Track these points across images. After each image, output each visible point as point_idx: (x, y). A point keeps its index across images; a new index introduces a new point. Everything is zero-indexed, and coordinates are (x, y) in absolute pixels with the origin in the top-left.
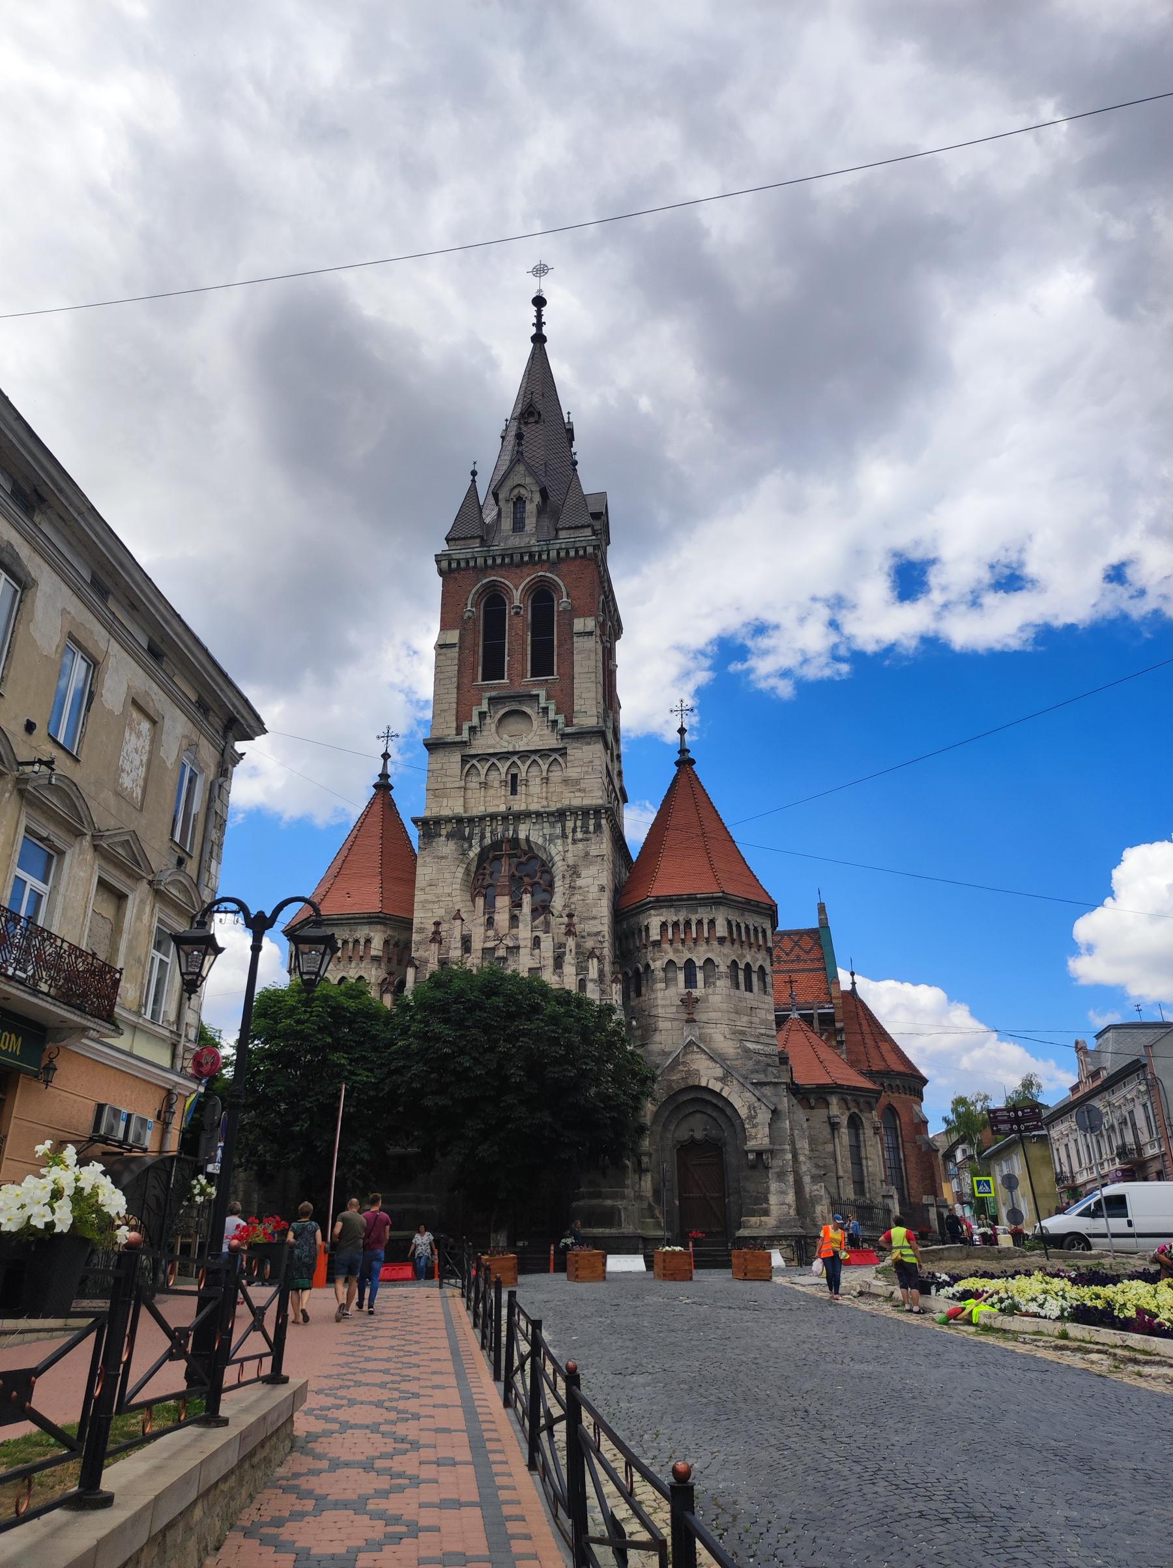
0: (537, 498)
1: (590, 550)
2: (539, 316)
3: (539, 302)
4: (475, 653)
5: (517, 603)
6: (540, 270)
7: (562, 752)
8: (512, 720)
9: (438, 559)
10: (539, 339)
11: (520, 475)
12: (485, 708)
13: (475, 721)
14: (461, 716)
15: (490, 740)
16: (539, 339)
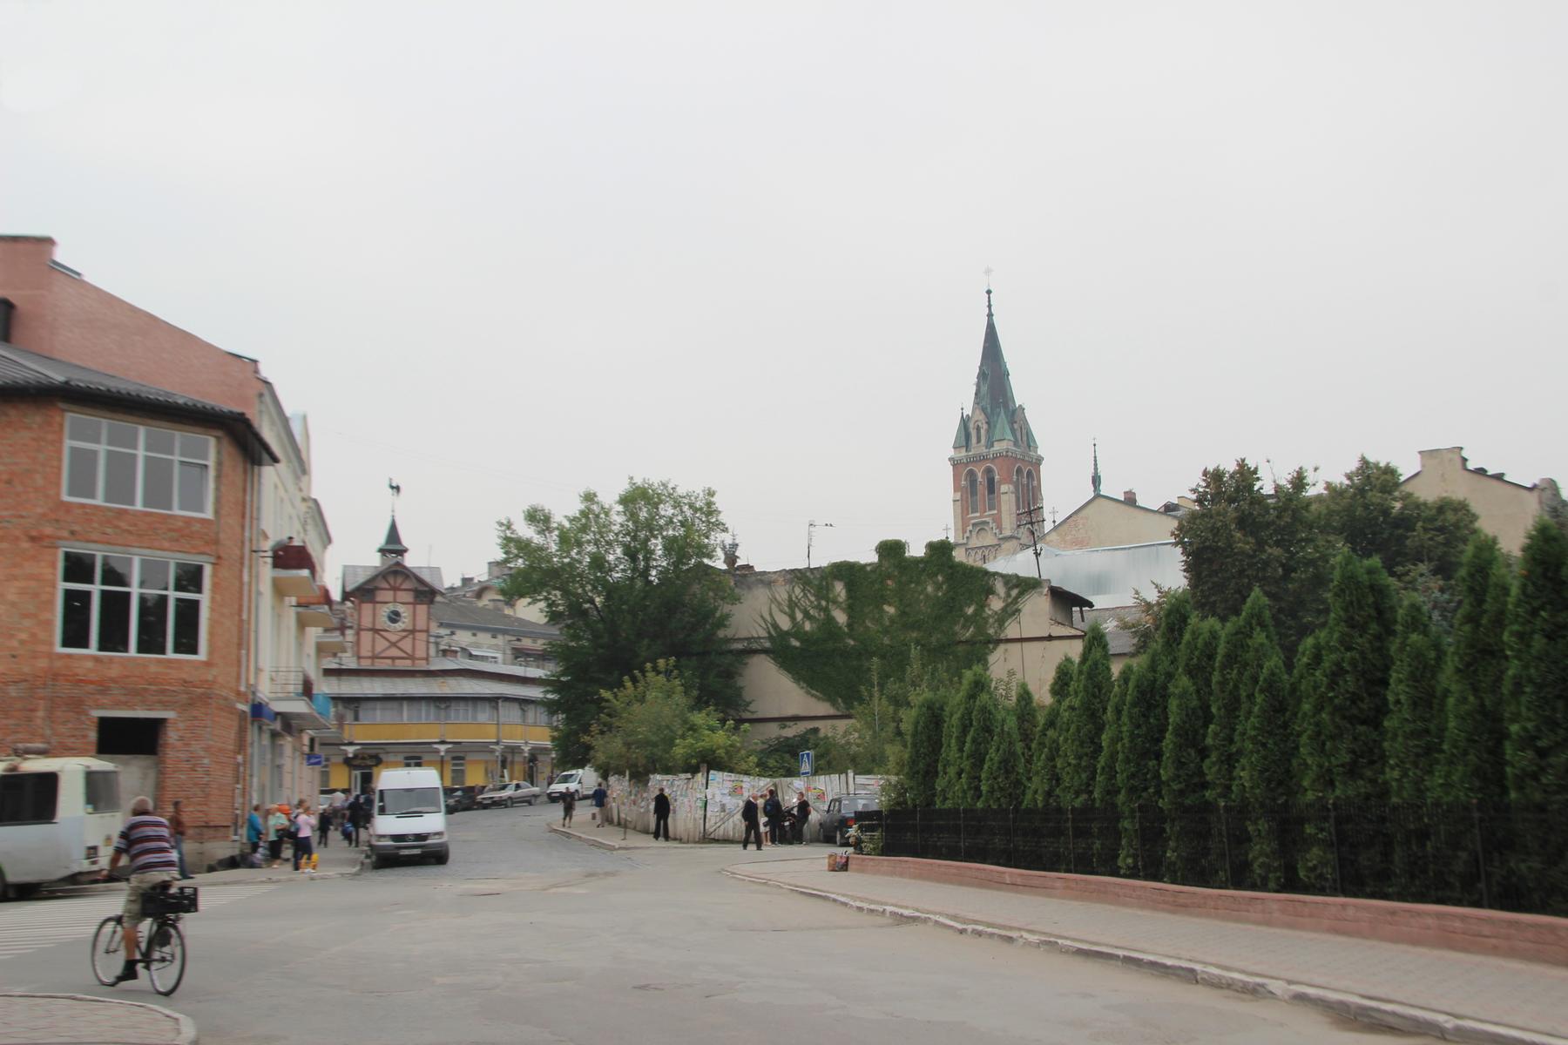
0: (985, 426)
1: (1004, 453)
2: (989, 301)
3: (989, 292)
4: (967, 502)
5: (980, 479)
6: (988, 271)
7: (999, 545)
8: (983, 532)
9: (950, 459)
10: (990, 315)
11: (981, 417)
12: (970, 528)
13: (968, 534)
14: (964, 532)
15: (974, 542)
16: (990, 315)
